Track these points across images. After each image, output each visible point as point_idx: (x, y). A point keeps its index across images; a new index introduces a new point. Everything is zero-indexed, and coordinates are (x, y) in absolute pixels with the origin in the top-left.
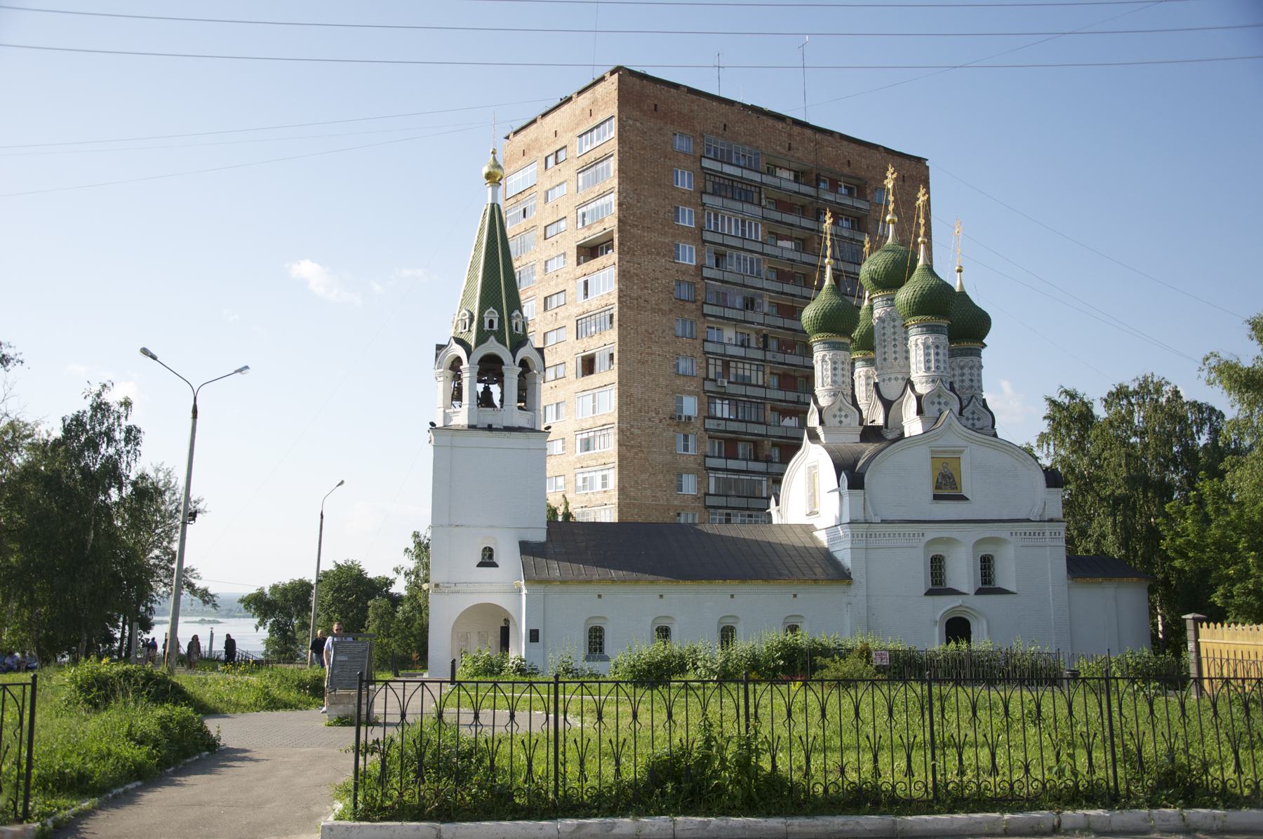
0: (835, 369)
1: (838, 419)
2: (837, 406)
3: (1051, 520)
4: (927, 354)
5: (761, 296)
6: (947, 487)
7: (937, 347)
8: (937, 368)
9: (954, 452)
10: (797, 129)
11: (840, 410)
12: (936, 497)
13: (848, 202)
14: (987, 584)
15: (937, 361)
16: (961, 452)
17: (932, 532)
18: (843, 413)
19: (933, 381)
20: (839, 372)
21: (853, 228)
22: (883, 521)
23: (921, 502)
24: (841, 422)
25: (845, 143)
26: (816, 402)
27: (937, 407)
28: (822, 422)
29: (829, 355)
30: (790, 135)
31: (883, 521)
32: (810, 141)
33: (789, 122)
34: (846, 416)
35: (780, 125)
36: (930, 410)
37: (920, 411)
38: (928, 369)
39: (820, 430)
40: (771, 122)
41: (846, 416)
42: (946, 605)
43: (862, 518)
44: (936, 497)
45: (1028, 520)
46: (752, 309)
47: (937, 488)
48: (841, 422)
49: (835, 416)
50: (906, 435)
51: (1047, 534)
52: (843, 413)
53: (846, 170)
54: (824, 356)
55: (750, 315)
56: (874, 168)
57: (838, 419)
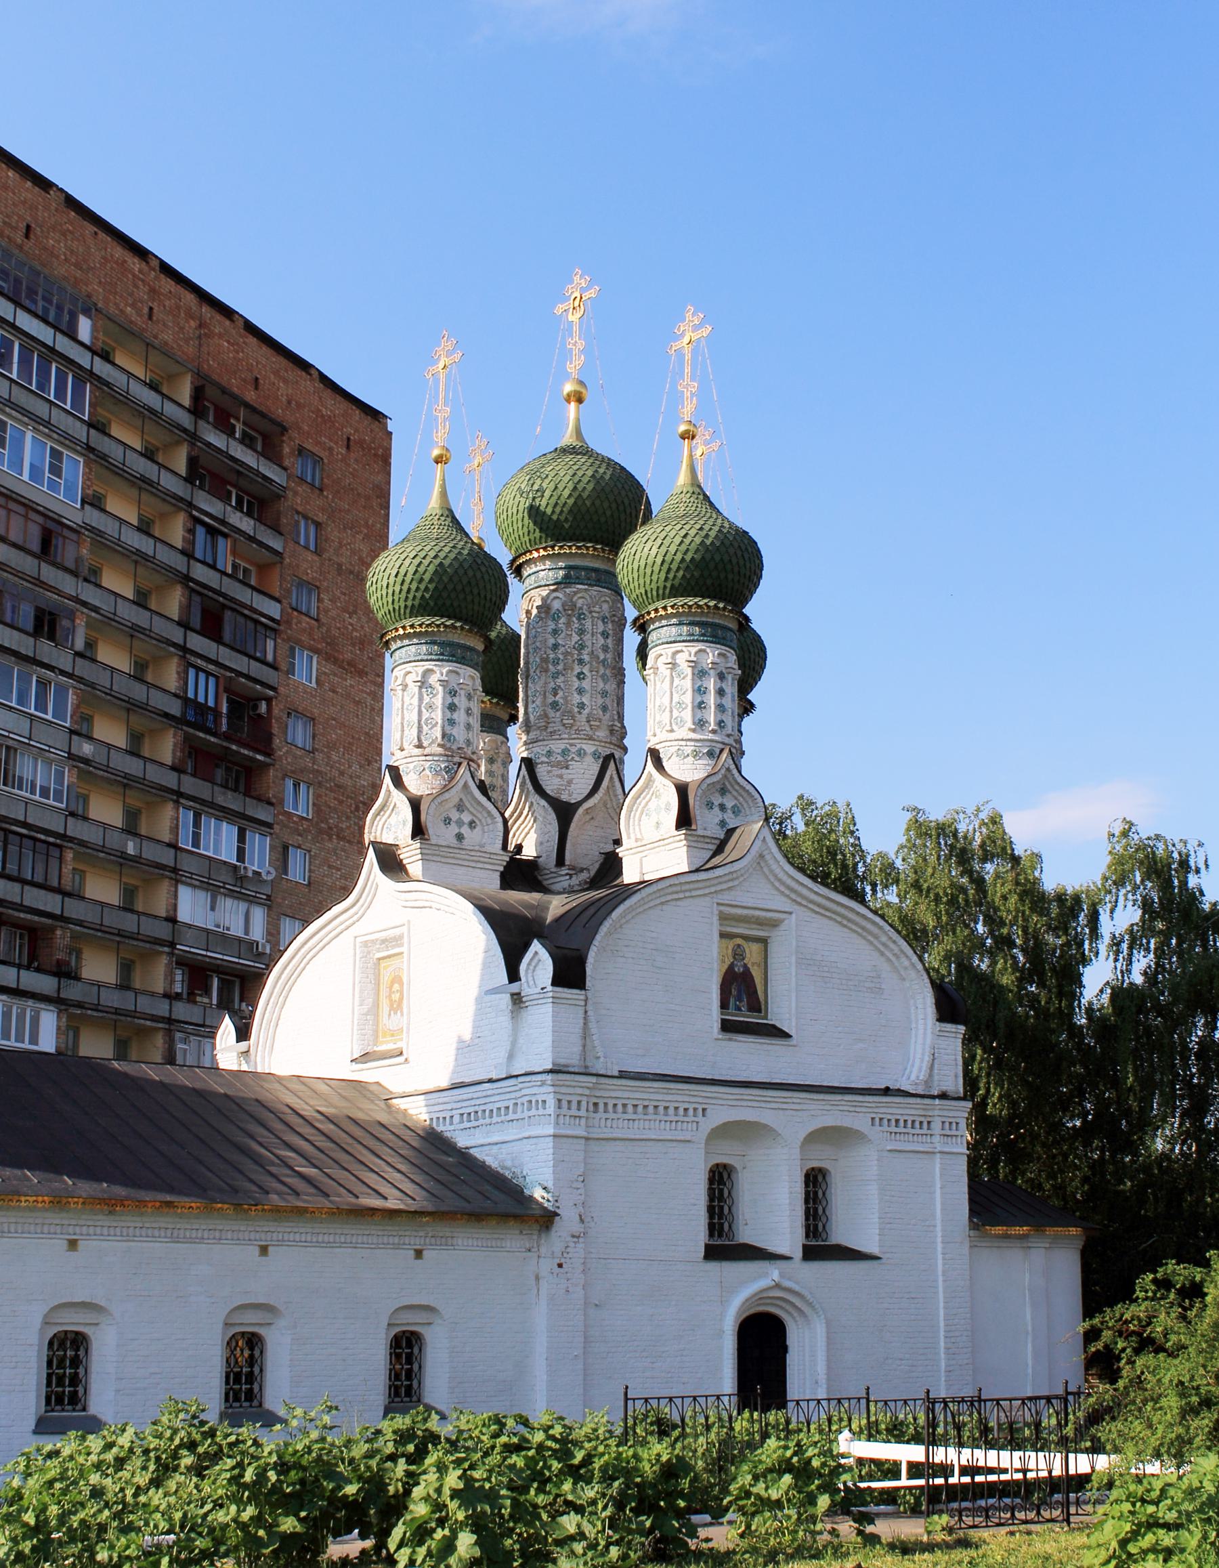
0: (452, 707)
1: (453, 829)
2: (454, 795)
3: (943, 1096)
4: (700, 691)
5: (72, 616)
6: (743, 1002)
7: (721, 676)
8: (721, 724)
9: (760, 922)
10: (168, 284)
11: (460, 807)
12: (728, 1027)
13: (249, 458)
14: (820, 1247)
15: (721, 708)
16: (775, 924)
17: (728, 1108)
18: (466, 818)
19: (710, 754)
20: (460, 716)
21: (249, 514)
22: (623, 1075)
23: (690, 1027)
24: (460, 837)
25: (252, 340)
26: (398, 782)
27: (715, 816)
28: (418, 831)
29: (440, 672)
30: (153, 291)
31: (623, 1075)
32: (190, 315)
33: (155, 263)
34: (472, 825)
35: (135, 264)
36: (708, 822)
37: (684, 820)
38: (700, 724)
39: (411, 853)
40: (119, 252)
41: (472, 825)
42: (745, 1287)
43: (574, 1061)
44: (728, 1027)
45: (901, 1093)
46: (51, 637)
47: (724, 1005)
48: (460, 837)
49: (447, 821)
50: (630, 875)
51: (936, 1126)
52: (466, 818)
53: (250, 396)
54: (428, 672)
55: (45, 649)
56: (299, 405)
57: (453, 829)
